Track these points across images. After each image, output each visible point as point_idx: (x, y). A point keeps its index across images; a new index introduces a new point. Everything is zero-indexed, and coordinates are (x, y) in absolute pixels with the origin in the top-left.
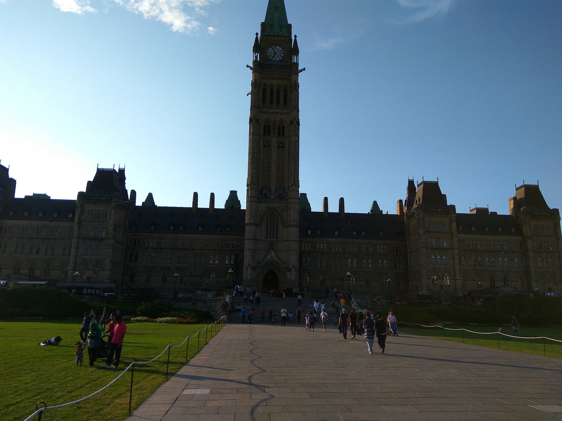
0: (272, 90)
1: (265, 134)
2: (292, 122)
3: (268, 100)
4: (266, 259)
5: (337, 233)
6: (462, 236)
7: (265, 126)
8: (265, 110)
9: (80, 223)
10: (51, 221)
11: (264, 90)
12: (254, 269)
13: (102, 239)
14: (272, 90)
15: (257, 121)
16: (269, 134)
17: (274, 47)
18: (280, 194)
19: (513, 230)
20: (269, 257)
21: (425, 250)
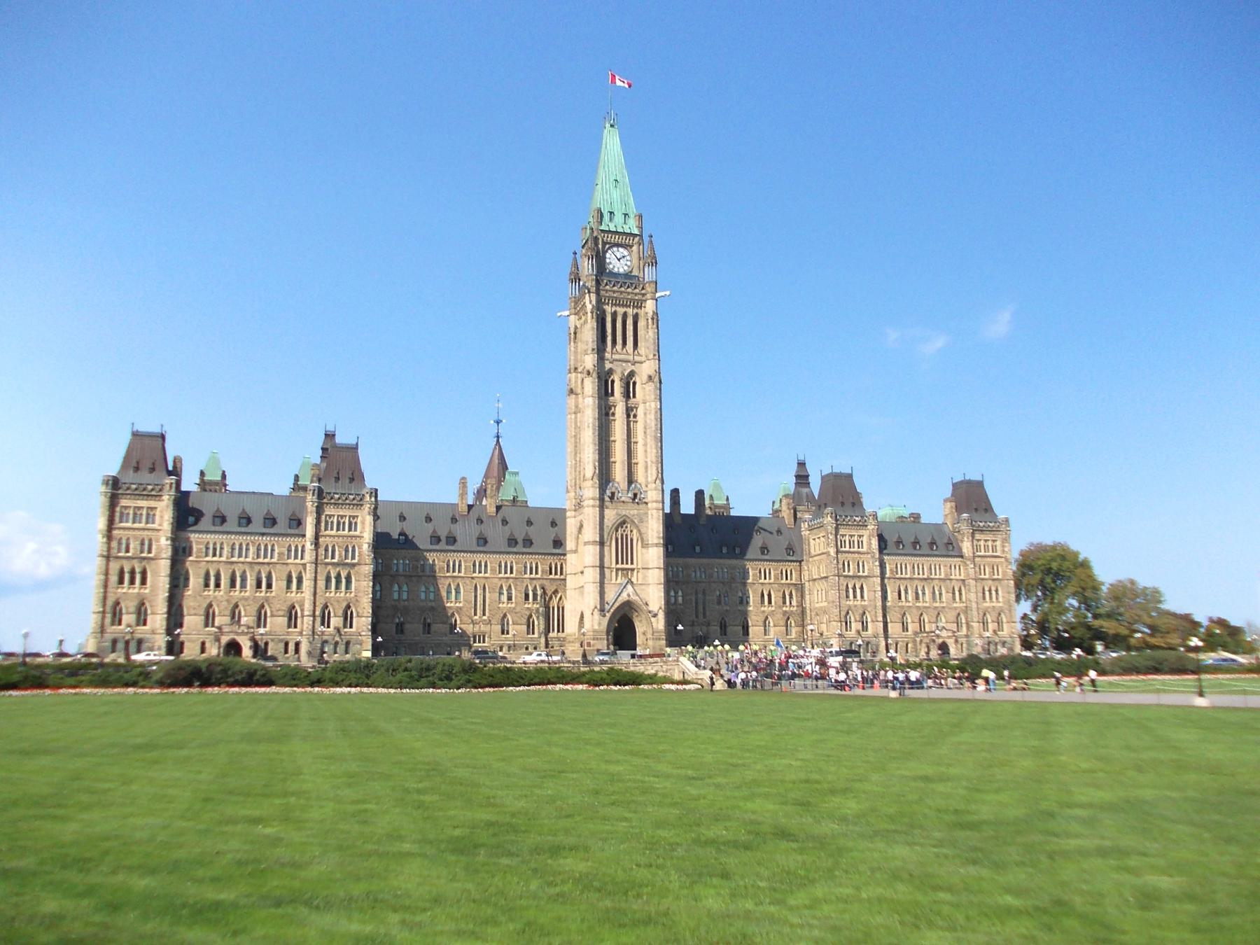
5: (698, 549)
9: (317, 537)
10: (263, 534)
13: (354, 565)
18: (635, 495)
20: (624, 595)
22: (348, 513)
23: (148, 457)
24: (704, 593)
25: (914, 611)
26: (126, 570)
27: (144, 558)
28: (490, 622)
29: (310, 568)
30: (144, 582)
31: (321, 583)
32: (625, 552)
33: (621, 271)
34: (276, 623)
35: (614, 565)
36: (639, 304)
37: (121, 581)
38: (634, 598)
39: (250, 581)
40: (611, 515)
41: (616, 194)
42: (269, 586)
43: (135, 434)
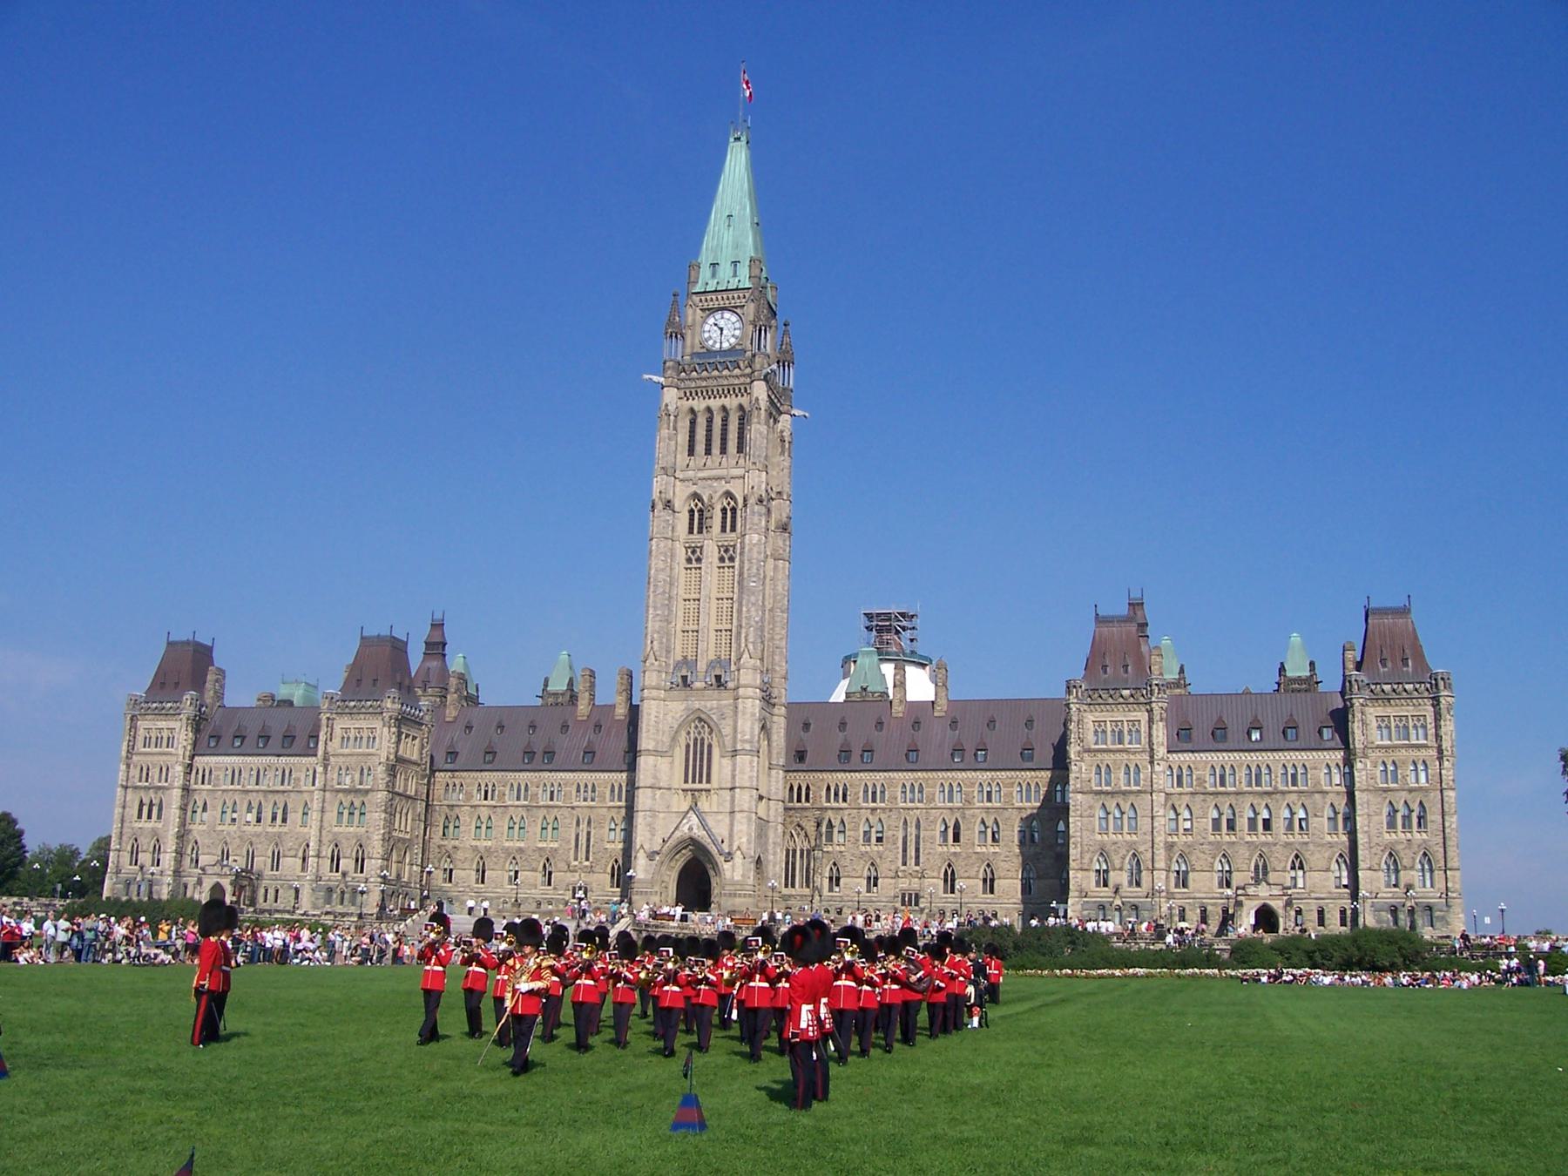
0: (710, 421)
1: (691, 531)
2: (745, 500)
3: (700, 447)
4: (678, 834)
6: (1187, 757)
7: (691, 512)
8: (691, 474)
11: (693, 423)
12: (651, 856)
13: (367, 792)
14: (710, 421)
15: (668, 504)
16: (700, 532)
17: (718, 315)
19: (1327, 734)
21: (1079, 796)
22: (364, 724)
23: (187, 668)
24: (918, 827)
25: (1244, 852)
26: (146, 801)
27: (160, 788)
28: (591, 870)
29: (317, 795)
30: (159, 817)
31: (331, 816)
32: (698, 765)
33: (726, 345)
34: (290, 864)
35: (678, 782)
36: (745, 390)
37: (140, 816)
38: (699, 833)
39: (267, 815)
40: (676, 709)
41: (728, 237)
42: (284, 820)
43: (170, 644)
